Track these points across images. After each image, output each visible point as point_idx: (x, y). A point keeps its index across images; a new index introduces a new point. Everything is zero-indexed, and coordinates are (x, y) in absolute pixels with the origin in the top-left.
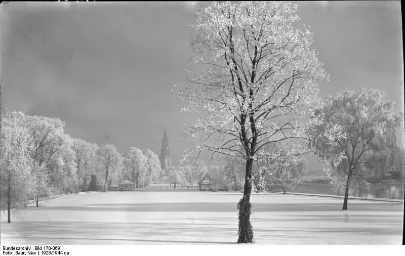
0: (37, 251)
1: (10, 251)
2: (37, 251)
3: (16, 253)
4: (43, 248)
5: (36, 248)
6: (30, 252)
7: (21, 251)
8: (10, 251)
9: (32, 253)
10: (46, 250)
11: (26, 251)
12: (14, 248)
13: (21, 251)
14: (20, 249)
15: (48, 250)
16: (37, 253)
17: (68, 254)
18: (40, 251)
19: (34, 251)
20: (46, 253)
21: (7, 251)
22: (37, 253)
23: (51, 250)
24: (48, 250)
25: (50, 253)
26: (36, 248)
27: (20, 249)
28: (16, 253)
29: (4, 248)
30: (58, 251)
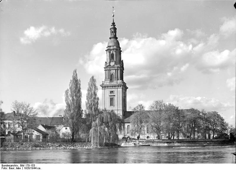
0: (21, 167)
1: (6, 167)
2: (22, 167)
3: (10, 168)
4: (25, 166)
5: (21, 166)
6: (17, 168)
7: (13, 167)
8: (6, 167)
9: (19, 168)
10: (27, 167)
11: (15, 167)
12: (8, 166)
13: (13, 167)
14: (12, 166)
15: (28, 167)
16: (22, 168)
17: (40, 169)
18: (24, 167)
19: (20, 167)
20: (27, 168)
21: (4, 167)
22: (22, 168)
23: (30, 167)
24: (28, 167)
25: (29, 168)
26: (21, 166)
27: (12, 166)
28: (10, 168)
29: (2, 165)
30: (34, 167)
